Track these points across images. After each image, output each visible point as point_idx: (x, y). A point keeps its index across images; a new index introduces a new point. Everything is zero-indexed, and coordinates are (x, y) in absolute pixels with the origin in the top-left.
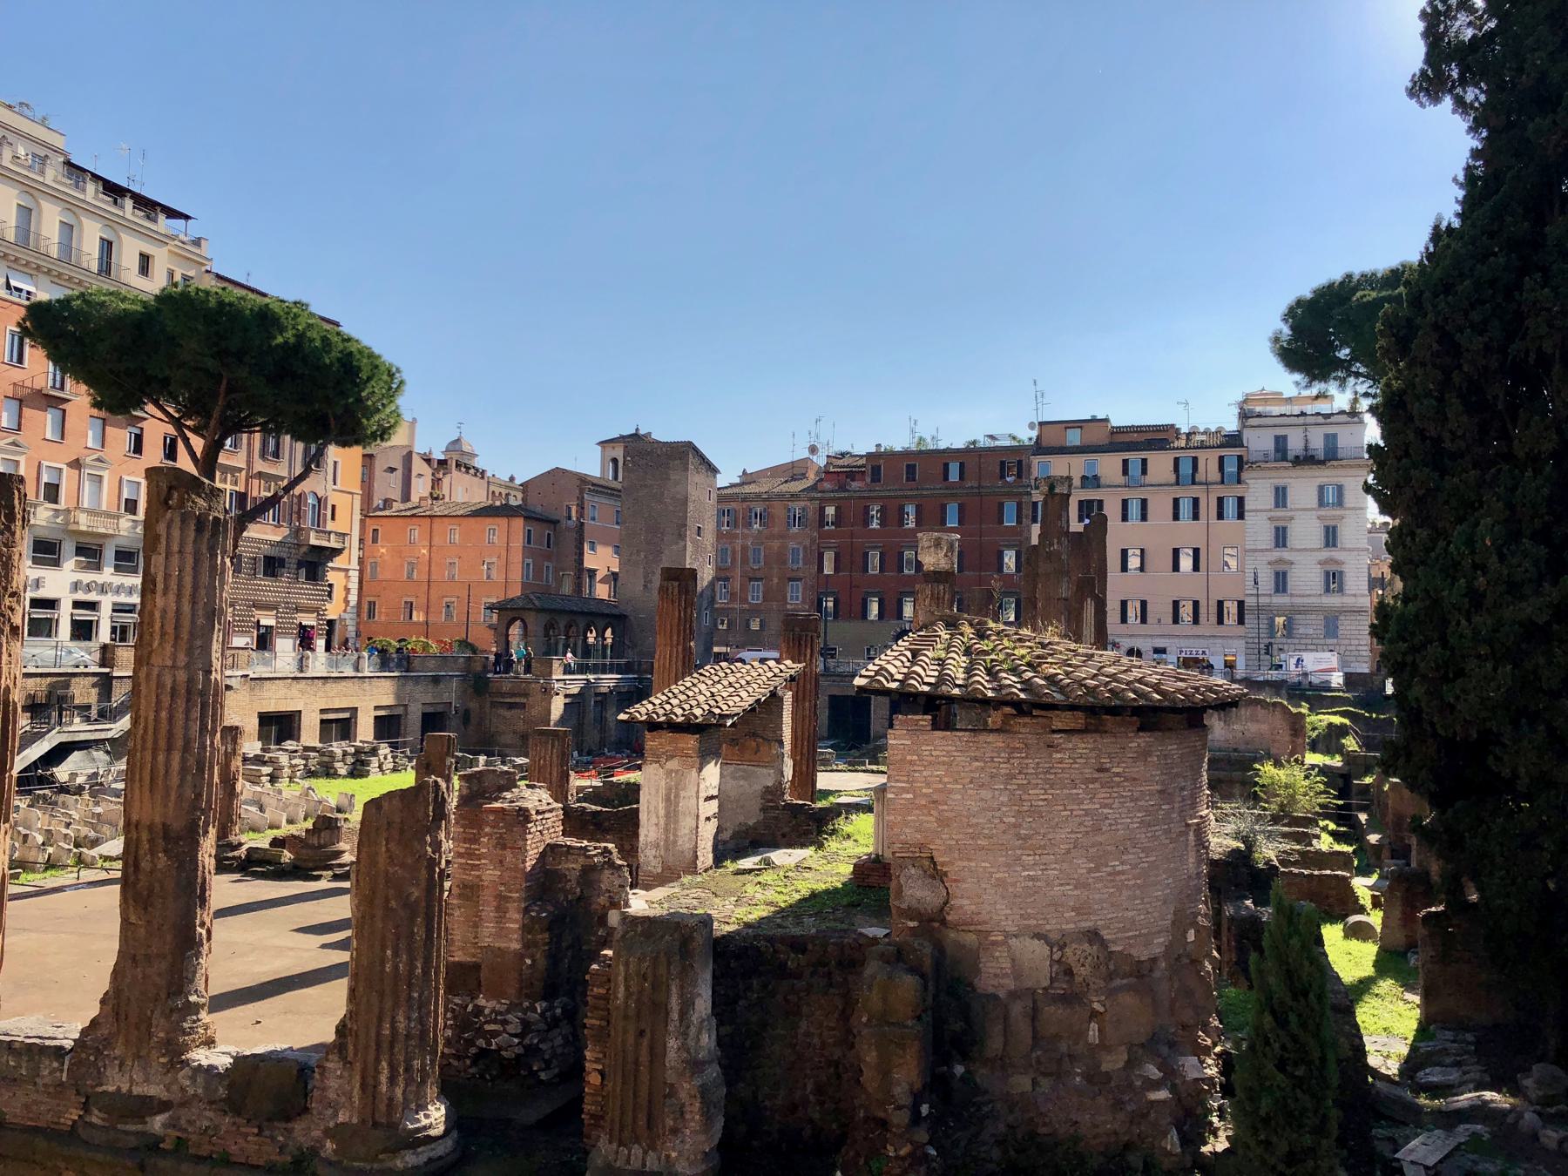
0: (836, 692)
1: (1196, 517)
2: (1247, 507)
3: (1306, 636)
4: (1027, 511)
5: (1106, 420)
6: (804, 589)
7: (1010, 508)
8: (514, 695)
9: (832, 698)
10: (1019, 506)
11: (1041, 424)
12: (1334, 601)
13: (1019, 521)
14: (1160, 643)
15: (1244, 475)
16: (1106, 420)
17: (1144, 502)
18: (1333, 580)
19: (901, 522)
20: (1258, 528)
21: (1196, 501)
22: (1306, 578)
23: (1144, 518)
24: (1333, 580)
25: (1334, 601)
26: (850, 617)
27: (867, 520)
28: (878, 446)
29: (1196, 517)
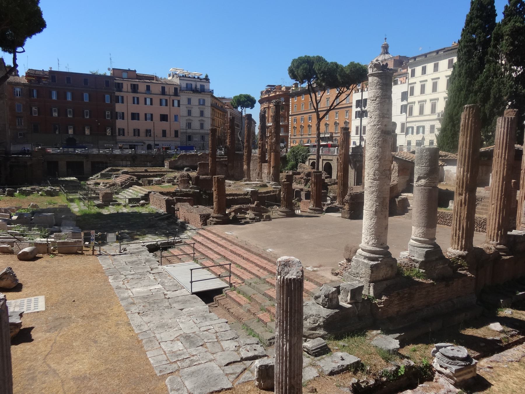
1: (166, 105)
3: (196, 141)
5: (135, 71)
11: (113, 69)
12: (201, 131)
13: (111, 101)
16: (135, 71)
17: (151, 100)
18: (202, 126)
19: (66, 98)
20: (183, 110)
21: (166, 100)
24: (202, 126)
27: (51, 97)
28: (51, 68)
29: (166, 105)
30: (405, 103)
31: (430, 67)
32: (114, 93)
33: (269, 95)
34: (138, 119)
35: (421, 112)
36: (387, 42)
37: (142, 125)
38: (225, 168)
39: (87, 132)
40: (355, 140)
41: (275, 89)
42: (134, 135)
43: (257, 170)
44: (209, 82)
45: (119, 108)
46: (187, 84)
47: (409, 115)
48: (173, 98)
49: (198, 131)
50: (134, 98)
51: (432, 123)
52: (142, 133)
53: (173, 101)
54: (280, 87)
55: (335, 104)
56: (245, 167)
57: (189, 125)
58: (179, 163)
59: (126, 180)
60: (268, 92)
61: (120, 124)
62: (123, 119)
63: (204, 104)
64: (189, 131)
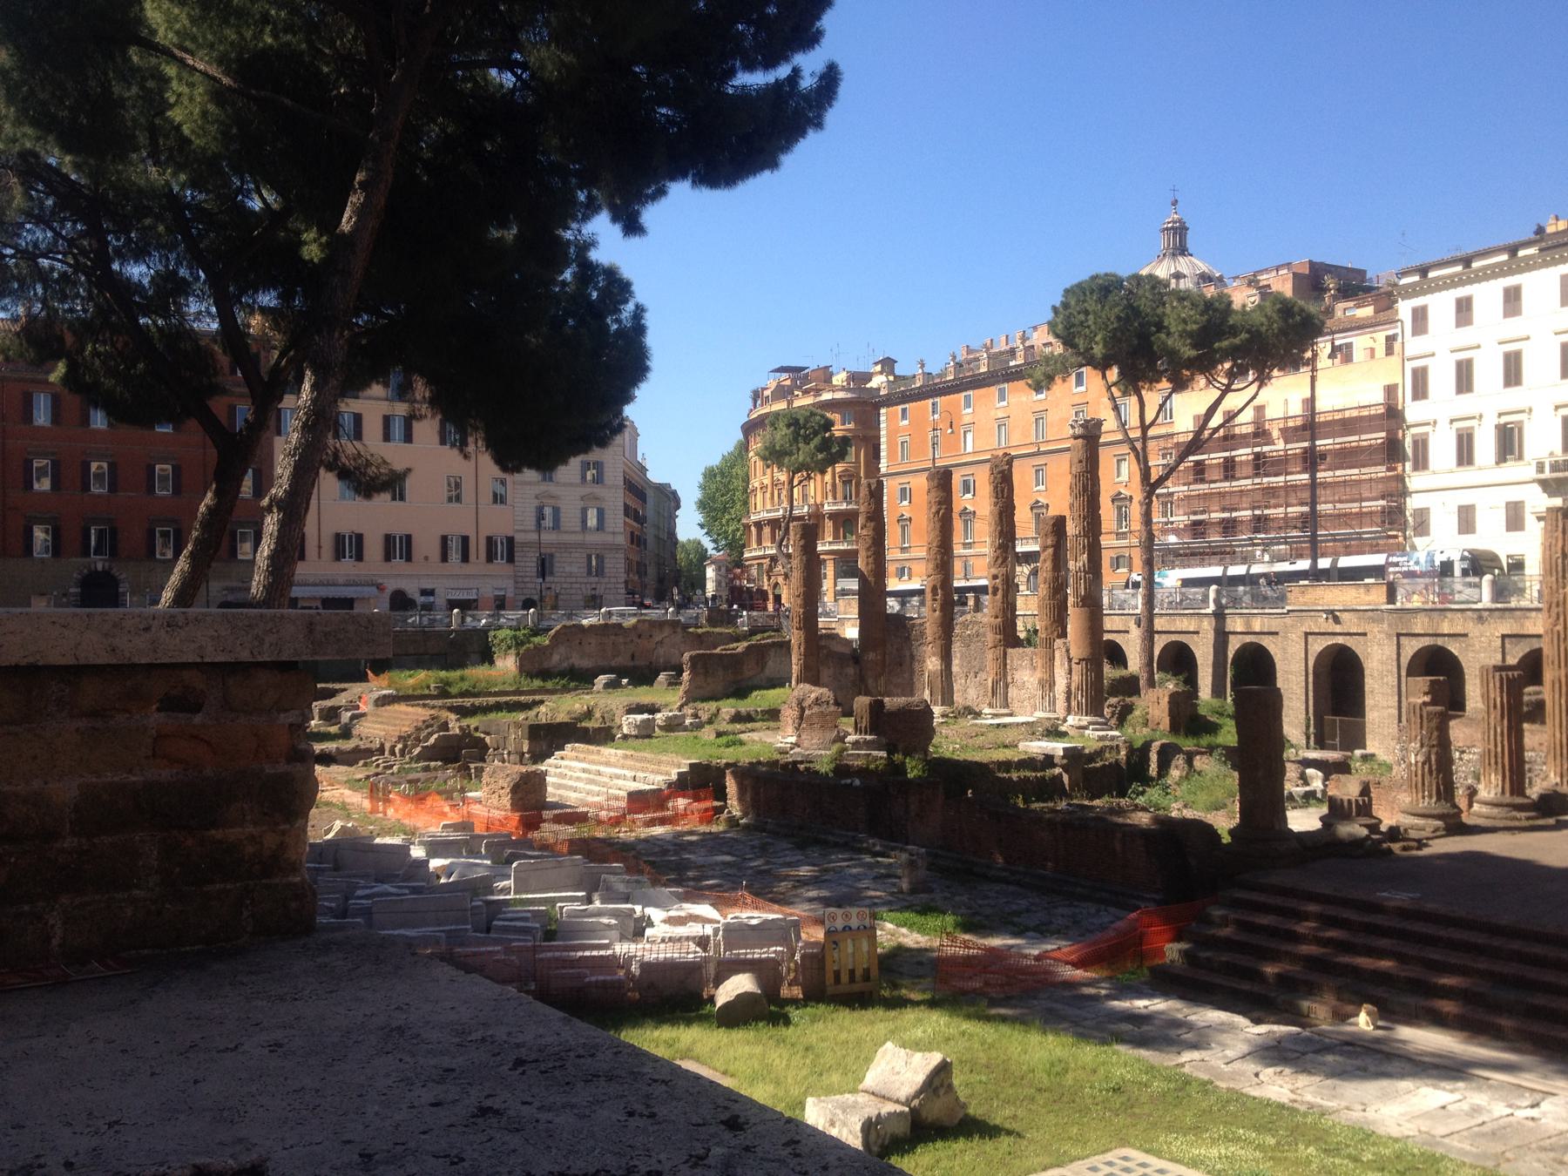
3: (571, 575)
27: (28, 416)
31: (1486, 295)
33: (790, 403)
35: (1465, 454)
36: (1184, 213)
38: (851, 671)
41: (806, 379)
43: (982, 676)
51: (1514, 494)
52: (374, 548)
54: (826, 375)
56: (932, 664)
58: (556, 658)
59: (418, 729)
60: (782, 392)
64: (547, 537)
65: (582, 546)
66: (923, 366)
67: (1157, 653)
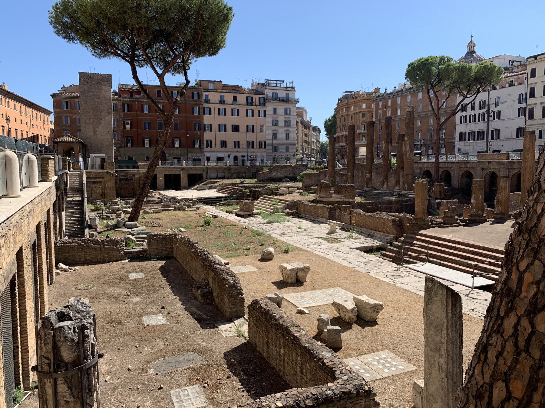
0: (167, 173)
2: (267, 113)
4: (202, 111)
5: (221, 82)
6: (118, 136)
7: (196, 109)
8: (96, 178)
9: (166, 176)
10: (199, 108)
11: (200, 81)
12: (287, 142)
13: (199, 114)
14: (243, 154)
15: (266, 104)
16: (221, 82)
17: (238, 110)
20: (269, 120)
21: (253, 111)
22: (281, 135)
23: (238, 115)
25: (287, 142)
26: (138, 146)
27: (143, 111)
29: (253, 116)
30: (523, 105)
32: (202, 104)
34: (238, 131)
37: (230, 137)
38: (344, 178)
39: (177, 145)
40: (460, 147)
42: (235, 147)
44: (295, 91)
45: (207, 119)
46: (273, 93)
47: (529, 119)
48: (259, 108)
49: (284, 141)
50: (219, 109)
53: (259, 111)
55: (435, 108)
57: (275, 135)
61: (207, 136)
62: (211, 131)
63: (289, 114)
64: (275, 141)
65: (284, 144)
66: (386, 90)
67: (440, 173)
